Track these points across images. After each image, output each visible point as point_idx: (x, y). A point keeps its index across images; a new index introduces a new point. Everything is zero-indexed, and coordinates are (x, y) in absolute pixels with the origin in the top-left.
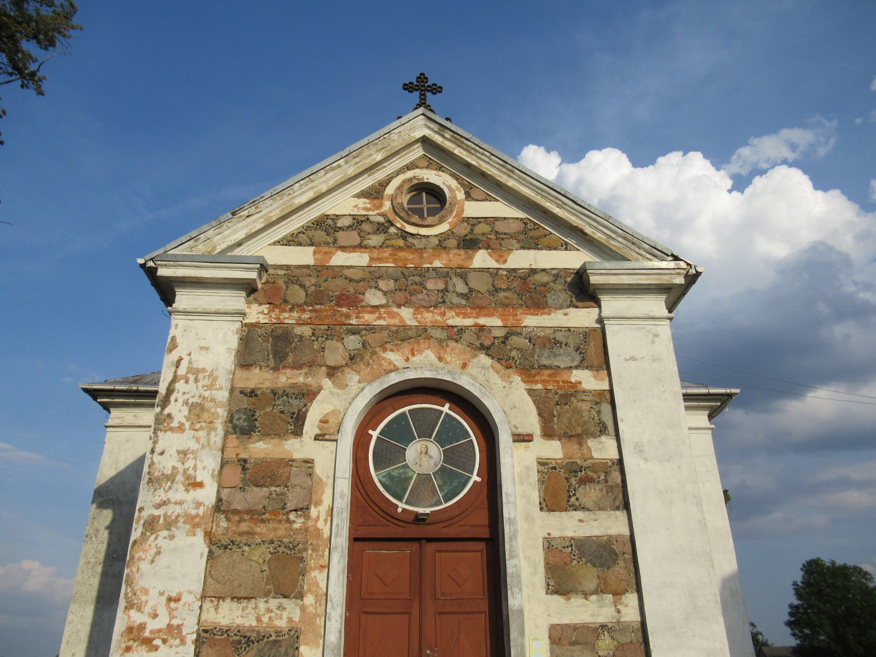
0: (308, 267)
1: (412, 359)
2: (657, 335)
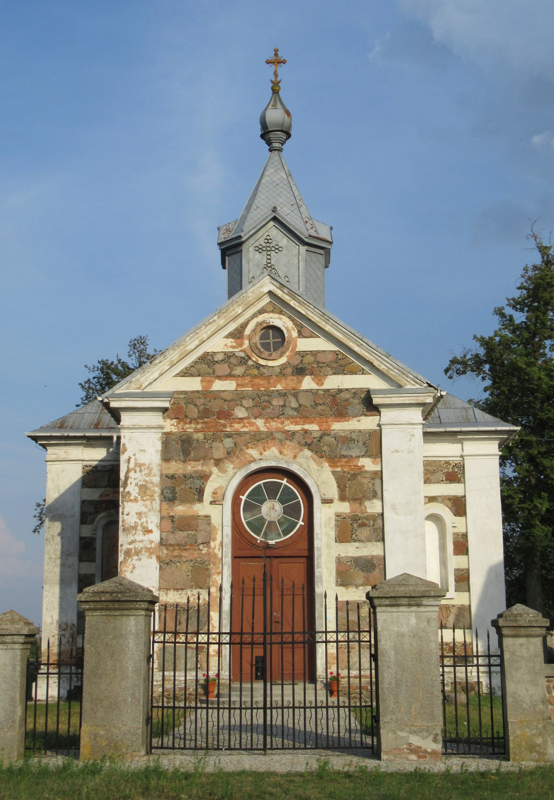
0: (198, 392)
1: (264, 453)
2: (413, 435)
